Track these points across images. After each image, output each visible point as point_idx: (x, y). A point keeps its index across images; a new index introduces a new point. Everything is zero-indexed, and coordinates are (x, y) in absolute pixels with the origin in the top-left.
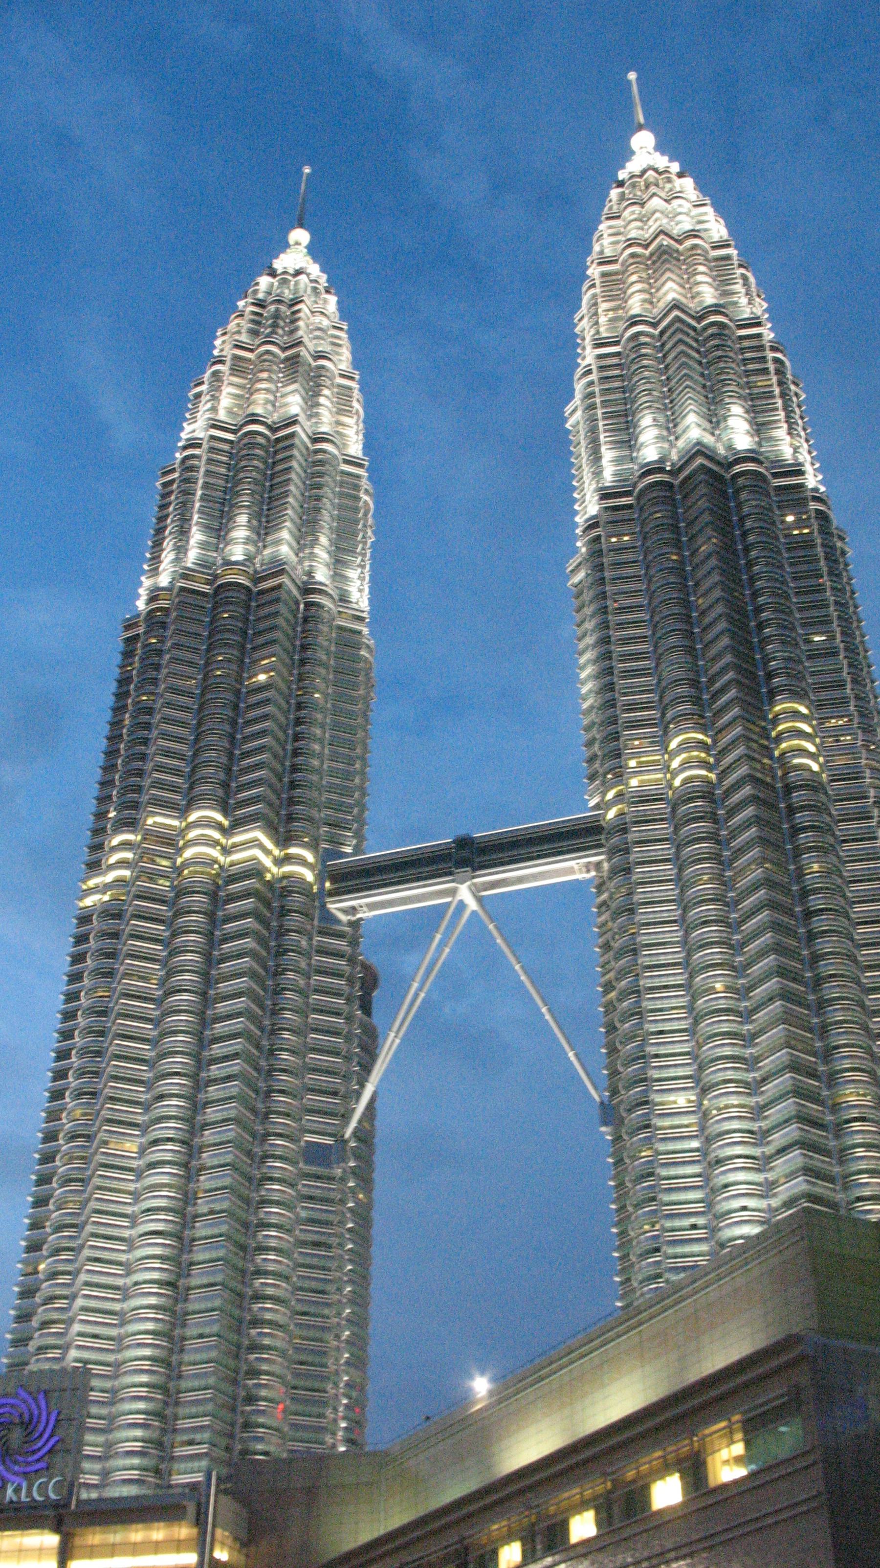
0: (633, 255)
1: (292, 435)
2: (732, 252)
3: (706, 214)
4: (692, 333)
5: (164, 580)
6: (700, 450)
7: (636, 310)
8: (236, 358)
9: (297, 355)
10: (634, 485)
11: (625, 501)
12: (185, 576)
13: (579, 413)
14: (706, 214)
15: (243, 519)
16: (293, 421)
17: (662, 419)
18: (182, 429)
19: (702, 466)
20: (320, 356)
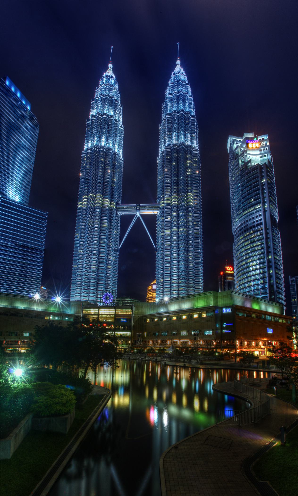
0: (175, 95)
1: (112, 119)
2: (192, 98)
3: (188, 87)
4: (184, 117)
5: (90, 146)
6: (183, 144)
7: (175, 109)
8: (101, 98)
9: (112, 100)
10: (171, 148)
11: (169, 150)
12: (94, 147)
13: (162, 126)
14: (188, 87)
15: (104, 136)
16: (112, 116)
17: (177, 135)
18: (90, 111)
19: (183, 147)
20: (116, 101)
